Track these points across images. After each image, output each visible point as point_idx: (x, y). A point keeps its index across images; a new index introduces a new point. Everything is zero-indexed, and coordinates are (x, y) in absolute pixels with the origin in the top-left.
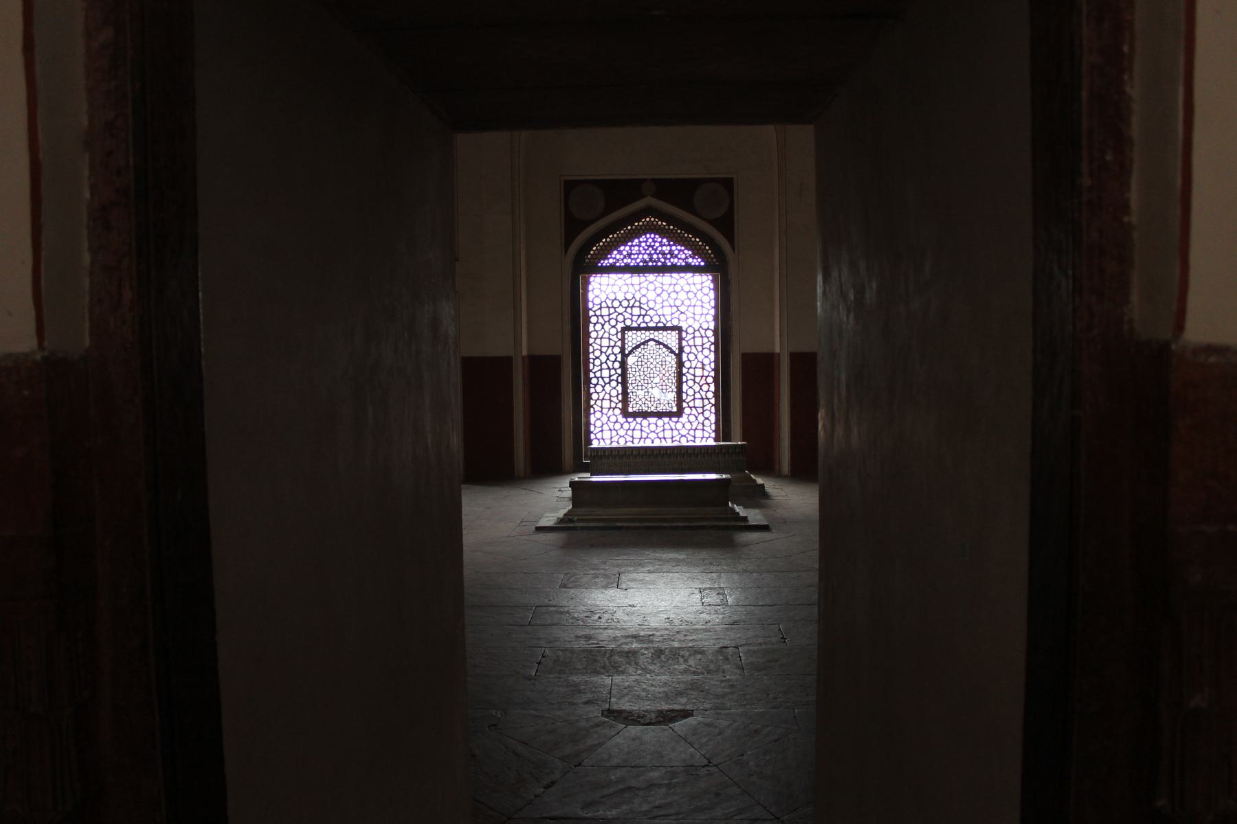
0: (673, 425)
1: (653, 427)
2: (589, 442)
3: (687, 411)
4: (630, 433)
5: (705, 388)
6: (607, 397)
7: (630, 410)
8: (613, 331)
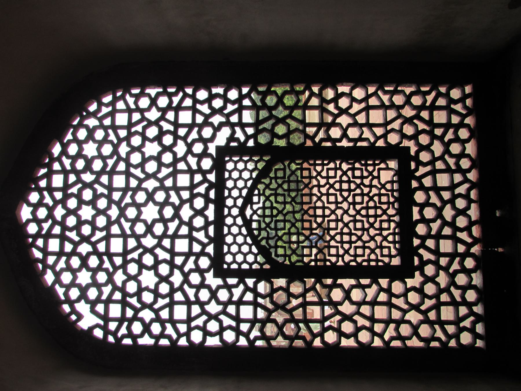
0: (422, 170)
1: (429, 213)
3: (393, 139)
4: (443, 261)
5: (344, 103)
6: (365, 310)
7: (396, 261)
8: (223, 295)
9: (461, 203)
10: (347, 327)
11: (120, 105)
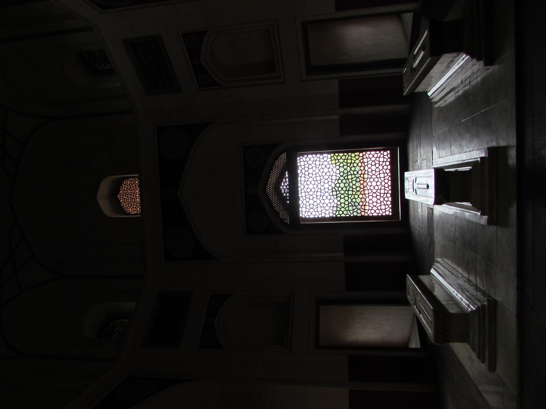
2: (387, 217)
4: (382, 195)
9: (386, 181)
10: (359, 211)
11: (301, 160)
